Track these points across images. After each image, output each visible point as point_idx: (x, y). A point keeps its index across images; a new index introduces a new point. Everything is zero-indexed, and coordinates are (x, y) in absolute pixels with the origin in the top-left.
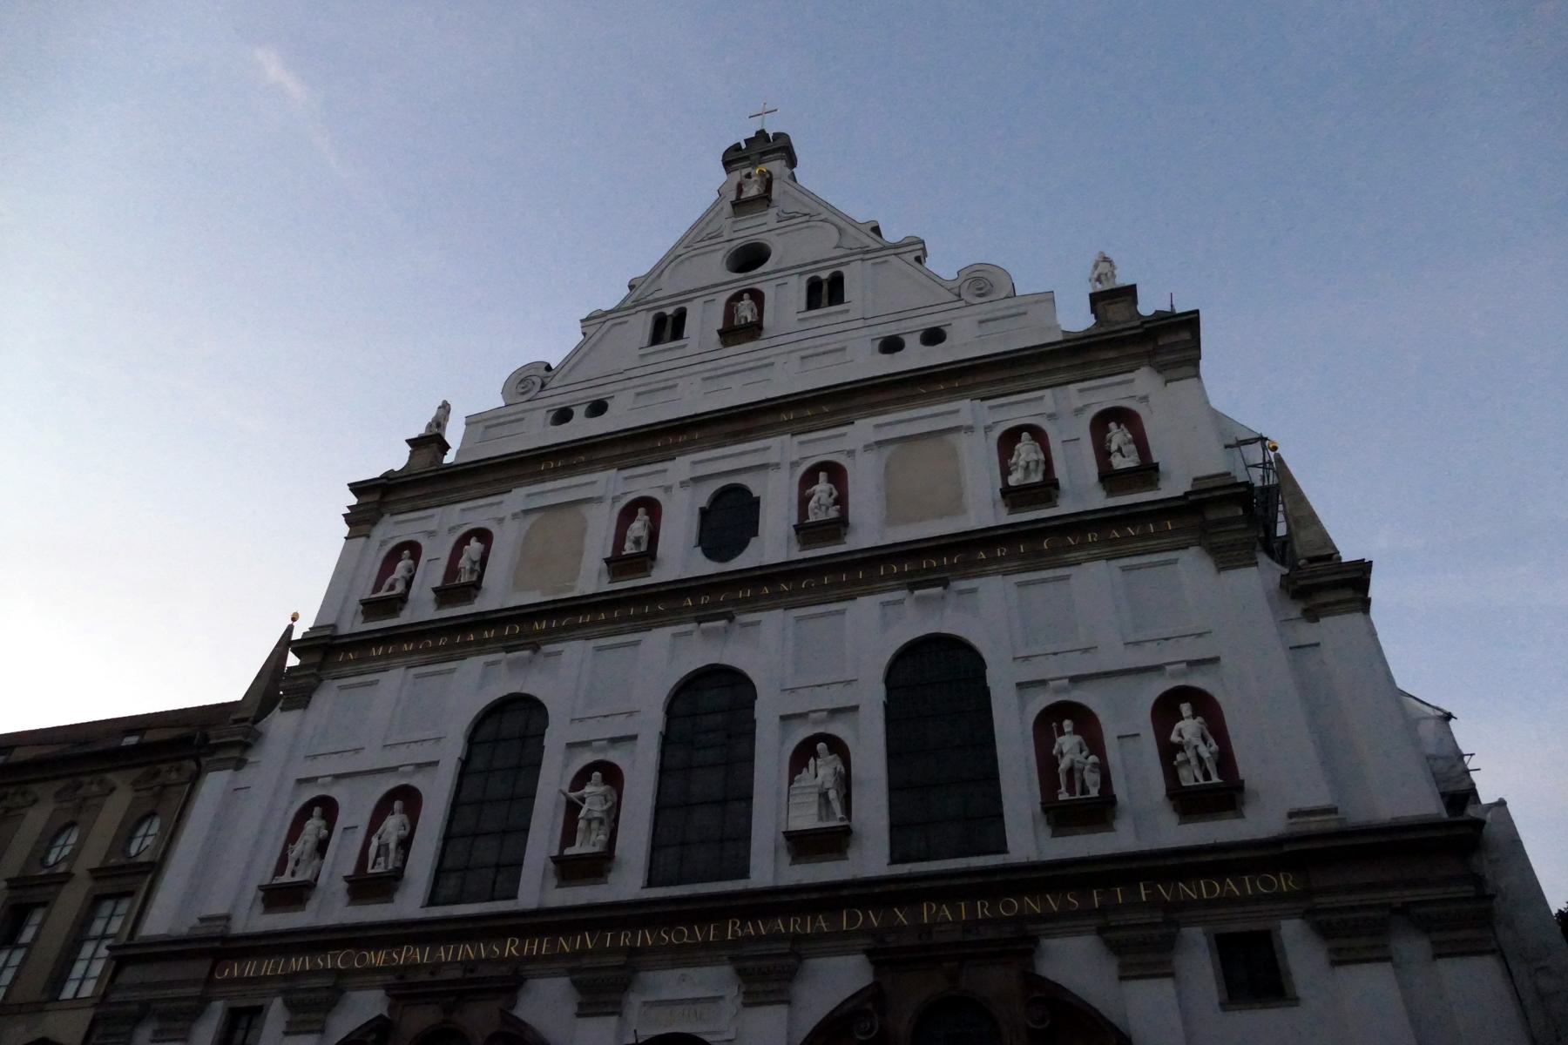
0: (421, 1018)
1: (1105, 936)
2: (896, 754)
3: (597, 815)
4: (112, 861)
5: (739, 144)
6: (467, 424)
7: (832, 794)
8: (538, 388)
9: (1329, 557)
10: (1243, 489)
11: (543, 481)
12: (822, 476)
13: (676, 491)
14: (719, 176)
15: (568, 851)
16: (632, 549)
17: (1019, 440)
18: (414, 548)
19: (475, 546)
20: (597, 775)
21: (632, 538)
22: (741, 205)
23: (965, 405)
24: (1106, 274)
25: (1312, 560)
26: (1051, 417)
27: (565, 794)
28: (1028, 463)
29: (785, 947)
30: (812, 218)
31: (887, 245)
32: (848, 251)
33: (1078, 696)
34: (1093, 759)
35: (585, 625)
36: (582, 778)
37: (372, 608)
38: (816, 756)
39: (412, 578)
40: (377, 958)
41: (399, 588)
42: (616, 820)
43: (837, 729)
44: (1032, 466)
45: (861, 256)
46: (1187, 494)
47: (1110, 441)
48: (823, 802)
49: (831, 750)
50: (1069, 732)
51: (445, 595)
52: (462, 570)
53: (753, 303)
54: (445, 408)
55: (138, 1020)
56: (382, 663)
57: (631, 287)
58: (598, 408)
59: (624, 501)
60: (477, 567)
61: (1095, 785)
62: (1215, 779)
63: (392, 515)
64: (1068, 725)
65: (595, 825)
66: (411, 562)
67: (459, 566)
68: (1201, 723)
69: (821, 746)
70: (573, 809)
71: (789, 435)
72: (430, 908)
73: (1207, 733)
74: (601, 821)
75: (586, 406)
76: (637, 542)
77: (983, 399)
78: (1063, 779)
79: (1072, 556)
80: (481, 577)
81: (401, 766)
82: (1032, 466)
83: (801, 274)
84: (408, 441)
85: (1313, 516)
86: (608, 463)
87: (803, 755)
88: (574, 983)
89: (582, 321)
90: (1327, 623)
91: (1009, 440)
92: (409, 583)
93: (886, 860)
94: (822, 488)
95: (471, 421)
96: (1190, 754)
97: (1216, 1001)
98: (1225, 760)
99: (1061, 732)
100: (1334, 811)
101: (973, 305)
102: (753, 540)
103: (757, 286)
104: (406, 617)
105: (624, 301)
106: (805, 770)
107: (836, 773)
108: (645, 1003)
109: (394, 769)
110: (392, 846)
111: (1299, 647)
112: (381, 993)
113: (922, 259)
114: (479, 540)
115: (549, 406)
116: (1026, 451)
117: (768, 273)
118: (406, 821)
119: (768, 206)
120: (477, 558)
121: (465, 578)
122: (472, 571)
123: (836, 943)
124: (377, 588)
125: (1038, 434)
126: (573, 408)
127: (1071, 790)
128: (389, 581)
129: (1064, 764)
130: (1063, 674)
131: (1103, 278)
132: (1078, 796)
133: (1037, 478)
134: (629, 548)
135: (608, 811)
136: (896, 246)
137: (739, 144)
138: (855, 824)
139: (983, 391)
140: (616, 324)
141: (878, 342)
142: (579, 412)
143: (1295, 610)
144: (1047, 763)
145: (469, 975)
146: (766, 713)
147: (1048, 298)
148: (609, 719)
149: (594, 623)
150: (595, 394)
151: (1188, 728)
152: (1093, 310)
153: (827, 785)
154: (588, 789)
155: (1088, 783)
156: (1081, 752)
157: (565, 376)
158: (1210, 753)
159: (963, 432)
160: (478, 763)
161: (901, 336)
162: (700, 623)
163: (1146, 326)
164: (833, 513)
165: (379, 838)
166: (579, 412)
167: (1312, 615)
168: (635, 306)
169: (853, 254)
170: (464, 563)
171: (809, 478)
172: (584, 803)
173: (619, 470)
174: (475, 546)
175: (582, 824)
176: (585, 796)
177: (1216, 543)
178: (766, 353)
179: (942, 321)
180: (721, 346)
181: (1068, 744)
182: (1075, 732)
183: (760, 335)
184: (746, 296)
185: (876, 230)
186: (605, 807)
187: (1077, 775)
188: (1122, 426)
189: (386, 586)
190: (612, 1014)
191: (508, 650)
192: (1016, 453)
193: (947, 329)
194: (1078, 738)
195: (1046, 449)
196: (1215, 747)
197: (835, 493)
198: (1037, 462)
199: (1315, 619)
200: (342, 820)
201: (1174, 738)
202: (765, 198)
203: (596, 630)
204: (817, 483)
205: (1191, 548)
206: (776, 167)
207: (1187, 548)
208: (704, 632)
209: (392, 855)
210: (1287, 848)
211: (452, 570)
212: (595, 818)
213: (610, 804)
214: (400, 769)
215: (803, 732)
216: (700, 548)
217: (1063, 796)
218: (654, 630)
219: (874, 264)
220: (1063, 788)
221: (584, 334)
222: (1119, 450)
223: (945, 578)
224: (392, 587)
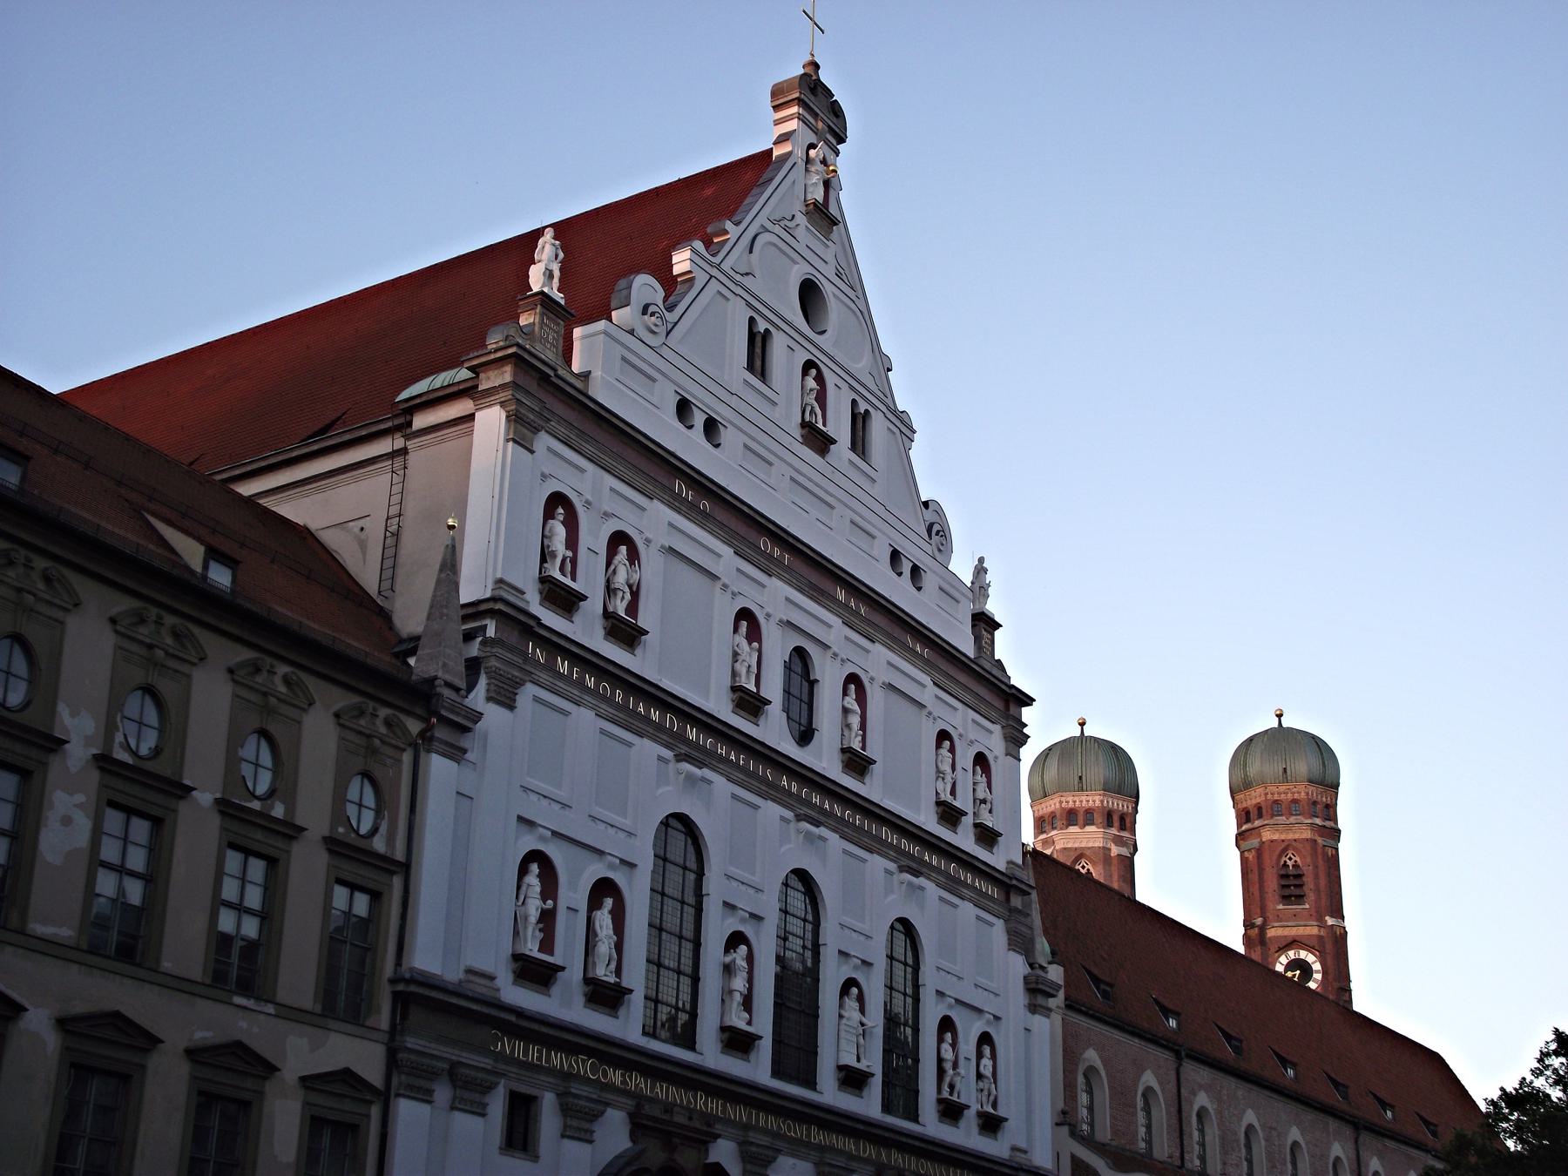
4: (341, 830)
23: (926, 679)
33: (958, 1016)
55: (432, 1075)
77: (935, 683)
83: (851, 387)
96: (986, 1087)
100: (1025, 1152)
150: (721, 412)
151: (986, 1063)
185: (889, 370)
219: (889, 429)
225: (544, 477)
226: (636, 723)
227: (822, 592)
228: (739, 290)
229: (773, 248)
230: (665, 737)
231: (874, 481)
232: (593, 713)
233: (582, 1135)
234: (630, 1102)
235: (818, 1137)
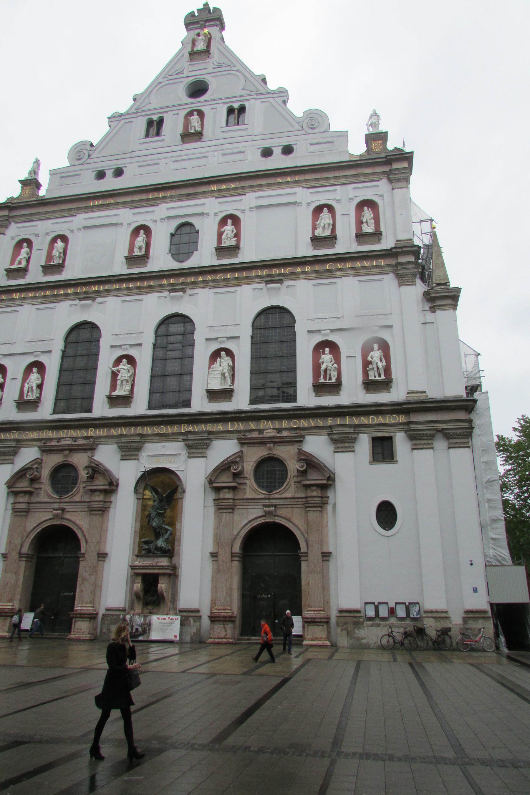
0: (55, 460)
1: (330, 436)
2: (254, 358)
3: (125, 378)
5: (194, 12)
6: (50, 175)
7: (227, 374)
8: (87, 157)
9: (445, 284)
10: (416, 249)
11: (92, 212)
12: (229, 221)
13: (158, 222)
14: (182, 33)
15: (114, 394)
16: (137, 252)
17: (322, 211)
18: (29, 243)
19: (60, 244)
20: (125, 361)
21: (137, 246)
22: (194, 55)
24: (375, 123)
25: (439, 285)
26: (339, 201)
27: (111, 369)
28: (325, 224)
29: (205, 436)
30: (232, 69)
31: (269, 91)
32: (249, 93)
33: (333, 338)
34: (336, 366)
35: (115, 289)
36: (118, 361)
37: (11, 273)
38: (220, 356)
39: (29, 258)
40: (34, 435)
41: (24, 264)
42: (134, 380)
43: (229, 345)
44: (326, 226)
45: (255, 97)
46: (392, 248)
47: (363, 217)
48: (222, 377)
49: (227, 355)
50: (327, 354)
51: (48, 269)
52: (55, 257)
53: (199, 118)
54: (37, 162)
56: (19, 302)
57: (135, 100)
58: (119, 172)
59: (134, 226)
60: (62, 255)
61: (334, 377)
62: (383, 377)
63: (15, 223)
64: (327, 350)
65: (124, 383)
66: (28, 249)
67: (53, 254)
68: (380, 353)
69: (223, 353)
70: (114, 375)
71: (214, 198)
72: (53, 415)
73: (382, 357)
74: (127, 381)
75: (113, 170)
76: (140, 248)
77: (308, 188)
78: (322, 373)
79: (338, 273)
80: (64, 261)
81: (34, 352)
82: (326, 226)
83: (224, 103)
84: (20, 181)
85: (443, 263)
86: (125, 204)
87: (216, 355)
88: (119, 447)
89: (109, 118)
90: (440, 314)
91: (318, 210)
92: (28, 260)
93: (248, 402)
94: (229, 228)
95: (53, 173)
96: (375, 366)
97: (368, 461)
98: (388, 370)
99: (324, 353)
101: (309, 134)
102: (195, 252)
103: (202, 108)
104: (29, 279)
105: (130, 108)
106: (215, 363)
107: (229, 366)
108: (148, 455)
109: (31, 353)
110: (34, 388)
111: (425, 323)
112: (37, 449)
113: (286, 101)
114: (62, 241)
115: (93, 169)
116: (325, 218)
117: (205, 101)
118: (39, 377)
119: (208, 57)
120: (61, 251)
121: (57, 261)
122: (60, 257)
123: (225, 434)
124: (12, 263)
125: (331, 209)
126: (106, 171)
127: (325, 378)
128: (18, 259)
129: (323, 367)
130: (328, 328)
131: (374, 125)
132: (327, 381)
133: (328, 233)
134: (137, 253)
135: (130, 376)
136: (273, 93)
137: (194, 12)
138: (235, 387)
139: (308, 184)
140: (126, 122)
141: (260, 150)
142: (109, 173)
143: (427, 306)
144: (317, 367)
145: (73, 443)
146: (199, 337)
147: (344, 135)
148: (129, 335)
149: (120, 289)
150: (117, 164)
151: (376, 355)
152: (367, 143)
153: (225, 370)
154: (121, 367)
155: (332, 376)
156: (331, 362)
157: (99, 153)
158: (382, 366)
159: (297, 205)
160: (70, 352)
161: (272, 148)
162: (170, 292)
163: (388, 157)
164: (233, 242)
165: (28, 384)
166: (109, 173)
167: (433, 309)
168: (137, 113)
169: (251, 95)
170: (55, 253)
171: (223, 222)
172: (119, 373)
173: (130, 208)
174: (60, 244)
175: (119, 382)
176: (120, 370)
177: (400, 273)
178: (203, 150)
179: (292, 141)
180: (181, 143)
181: (327, 358)
182: (330, 353)
183: (201, 139)
184: (195, 113)
186: (129, 375)
187: (328, 372)
188: (370, 210)
189: (17, 262)
190: (135, 459)
191: (80, 299)
192: (320, 218)
193: (294, 147)
194: (331, 356)
195: (334, 217)
196: (384, 364)
197: (235, 231)
198: (329, 224)
199: (434, 312)
200: (9, 376)
201: (369, 359)
202: (207, 52)
203: (121, 293)
204: (227, 225)
205: (389, 274)
206: (214, 31)
207: (388, 274)
208: (172, 298)
209: (35, 391)
210: (404, 406)
211: (50, 256)
212: (124, 380)
213: (131, 373)
214: (34, 353)
215: (215, 346)
216: (170, 254)
217: (322, 380)
218: (149, 294)
219: (261, 102)
220: (322, 377)
221: (110, 126)
222: (367, 222)
223: (282, 280)
224: (20, 263)
225: (13, 238)
226: (55, 299)
227: (194, 194)
228: (138, 114)
229: (168, 86)
230: (73, 297)
231: (246, 129)
232: (30, 305)
233: (6, 462)
234: (39, 443)
235: (184, 428)
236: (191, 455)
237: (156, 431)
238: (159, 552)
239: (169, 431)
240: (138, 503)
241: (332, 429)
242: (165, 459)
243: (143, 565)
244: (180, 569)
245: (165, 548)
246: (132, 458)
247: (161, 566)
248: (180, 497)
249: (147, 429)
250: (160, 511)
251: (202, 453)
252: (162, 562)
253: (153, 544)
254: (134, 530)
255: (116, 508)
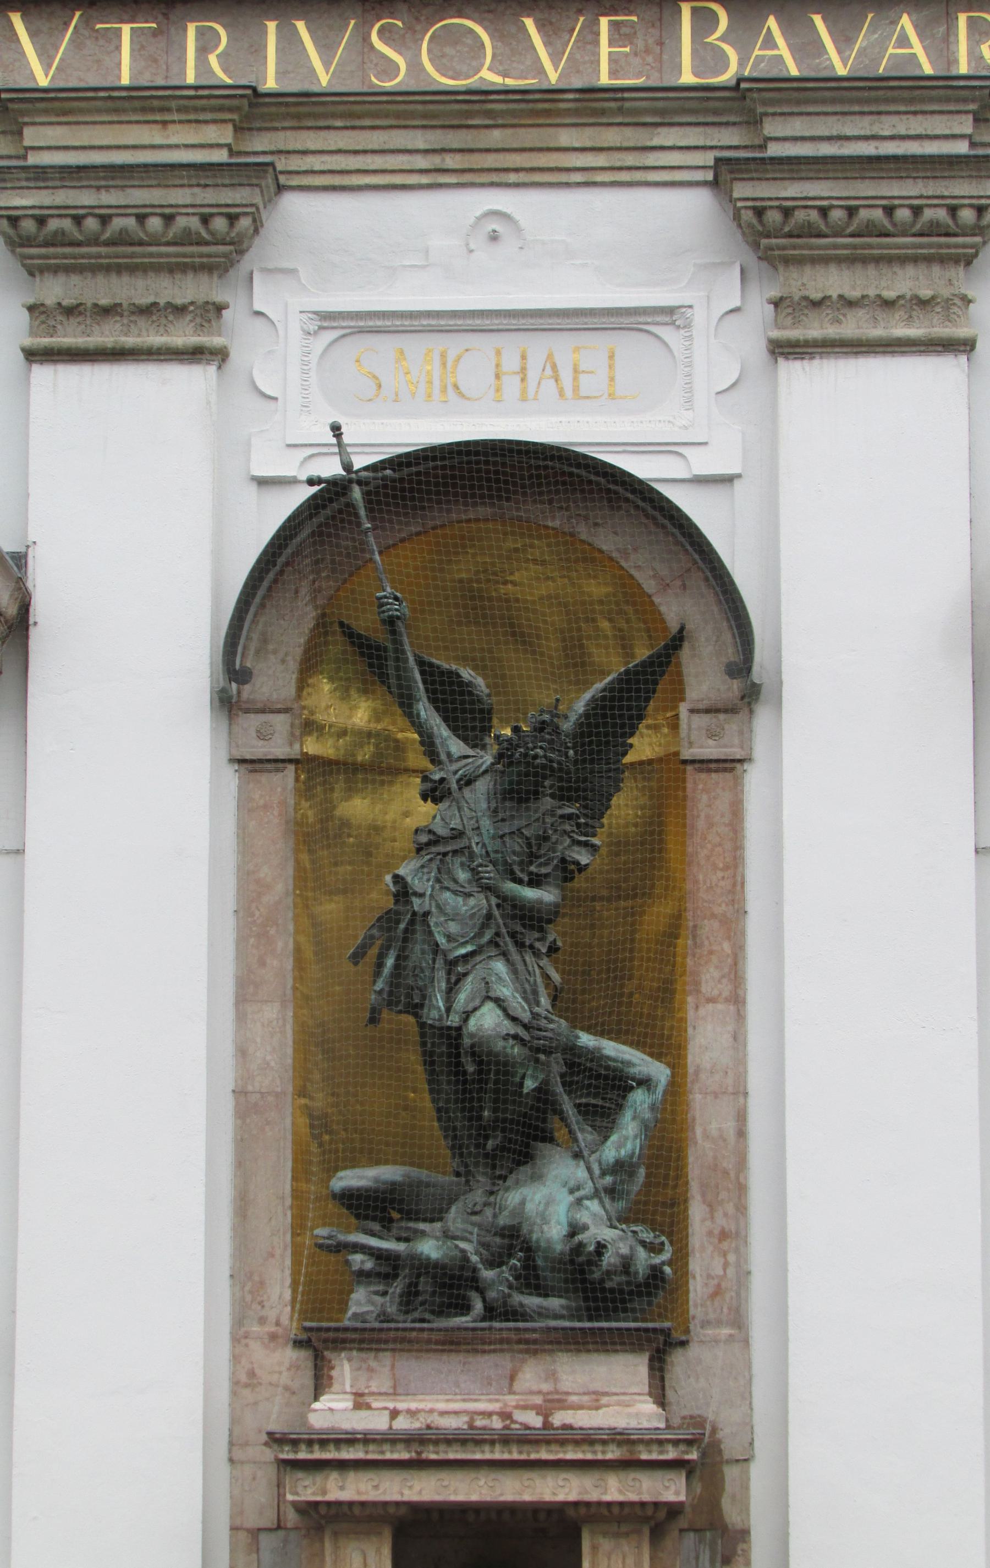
108: (327, 318)
190: (195, 354)
236: (815, 329)
237: (390, 69)
238: (555, 1303)
239: (541, 71)
240: (245, 807)
241: (754, 122)
242: (511, 362)
243: (402, 1424)
244: (758, 1474)
245: (626, 1264)
246: (156, 339)
247: (620, 1437)
248: (710, 750)
249: (289, 40)
250: (530, 894)
251: (924, 304)
252: (596, 1400)
253: (455, 1218)
254: (228, 1081)
255: (20, 852)
